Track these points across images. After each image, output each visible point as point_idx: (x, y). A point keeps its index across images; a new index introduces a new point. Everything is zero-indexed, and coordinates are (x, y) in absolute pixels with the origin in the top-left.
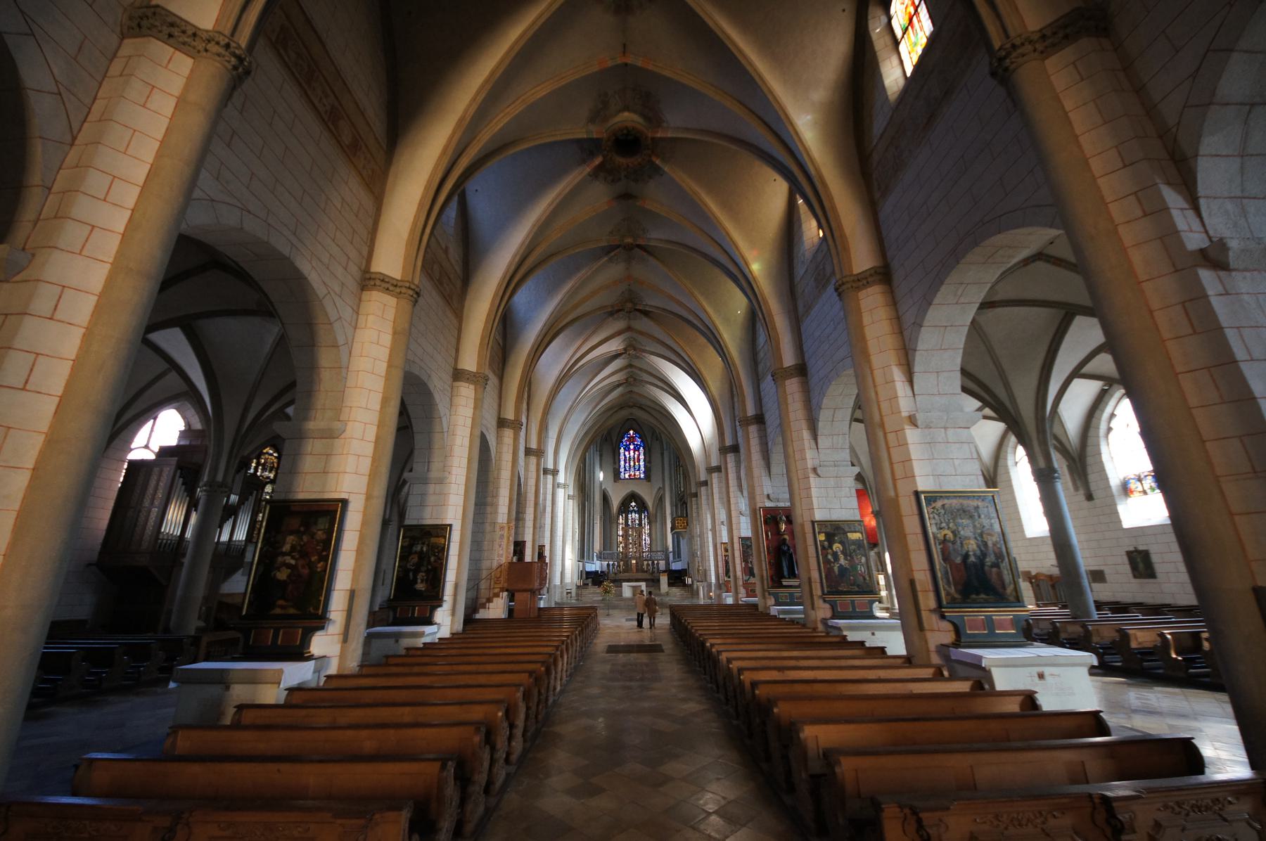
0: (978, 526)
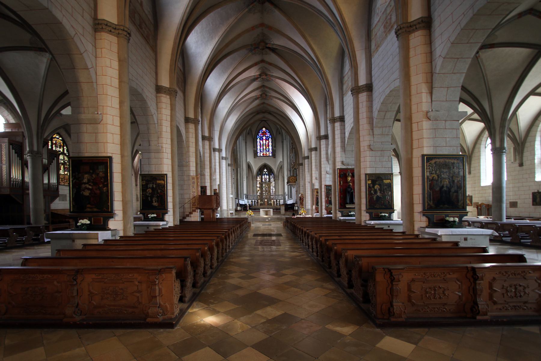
0: (452, 172)
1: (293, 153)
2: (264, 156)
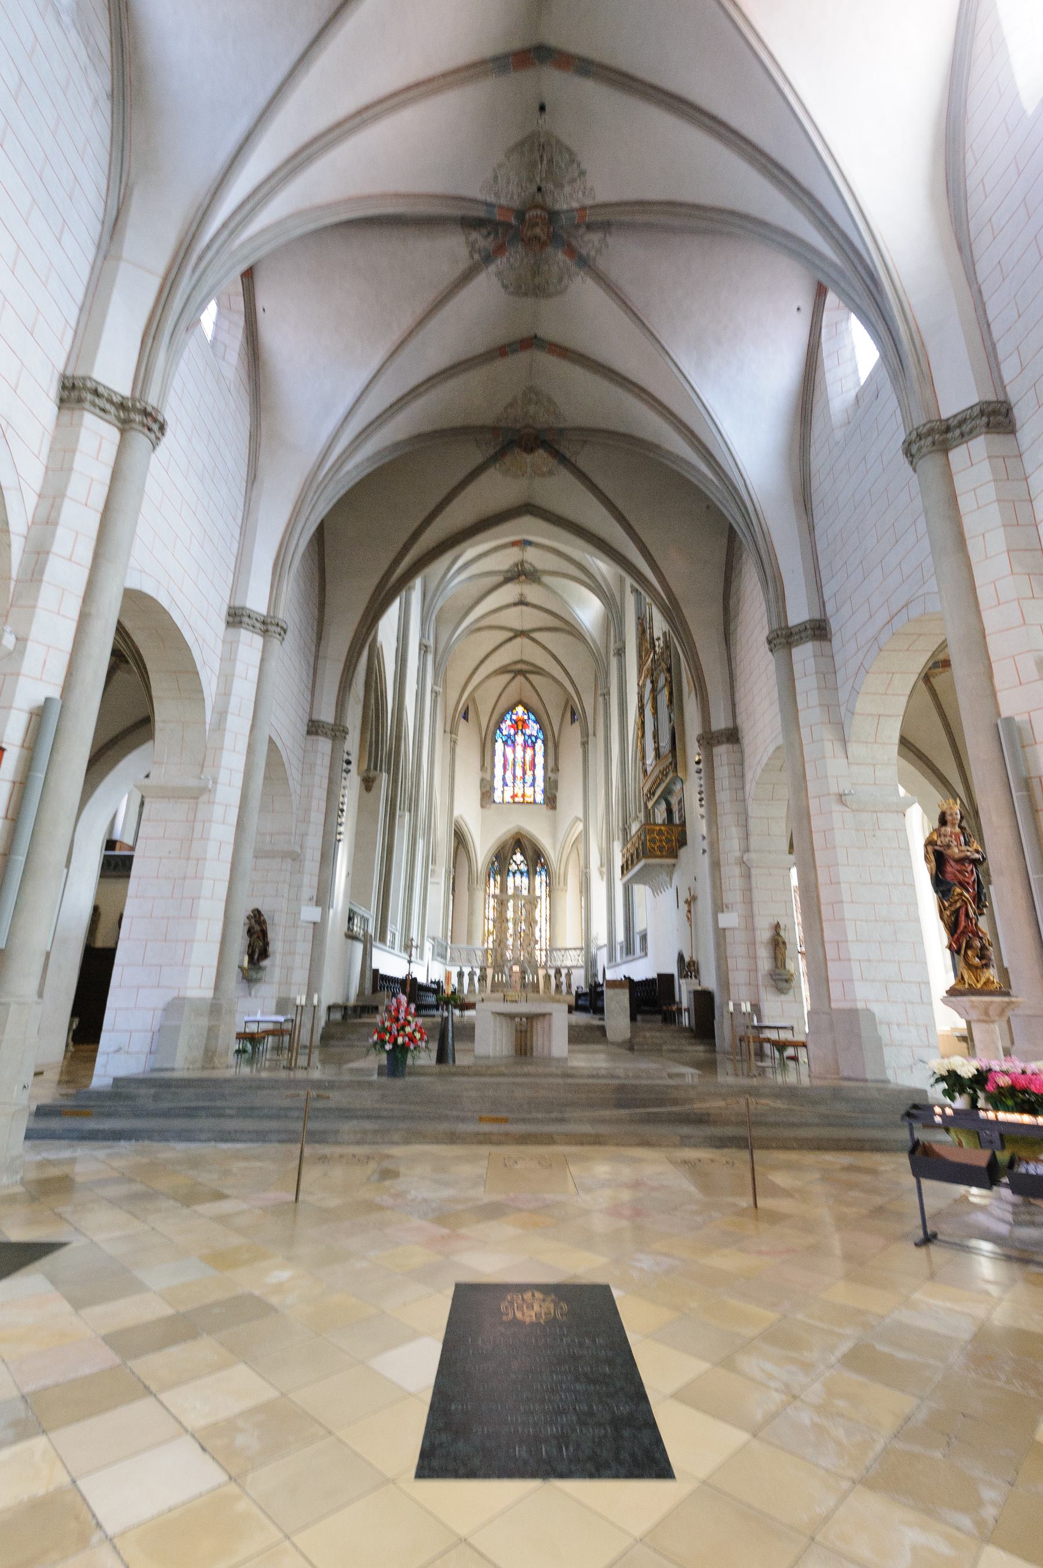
1: (655, 713)
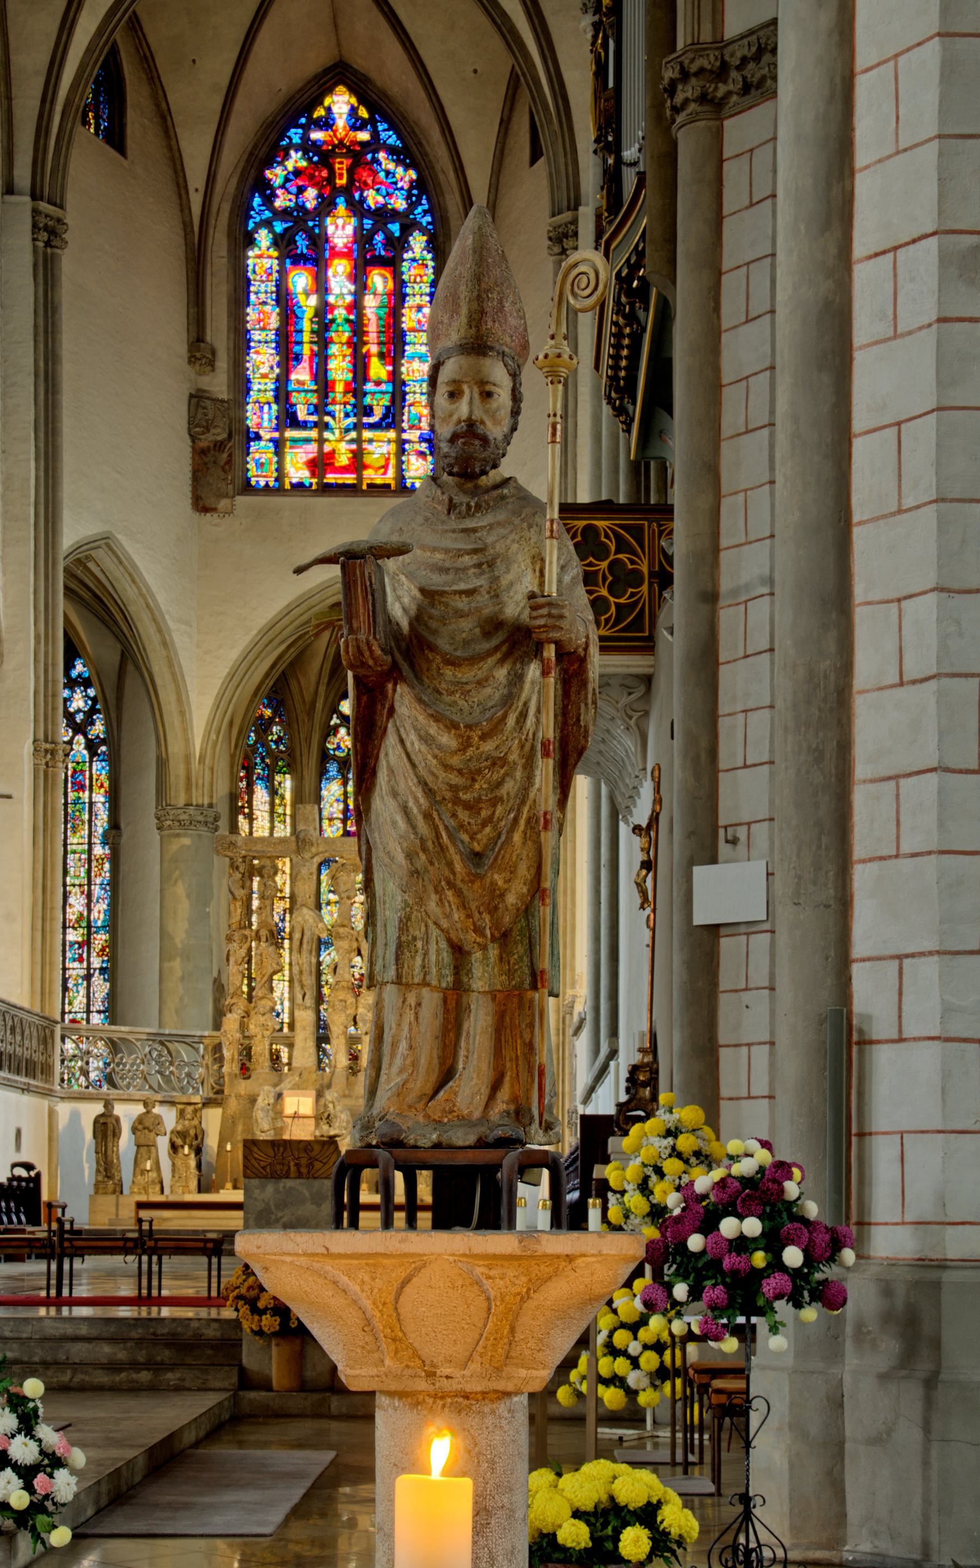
2: (327, 489)
